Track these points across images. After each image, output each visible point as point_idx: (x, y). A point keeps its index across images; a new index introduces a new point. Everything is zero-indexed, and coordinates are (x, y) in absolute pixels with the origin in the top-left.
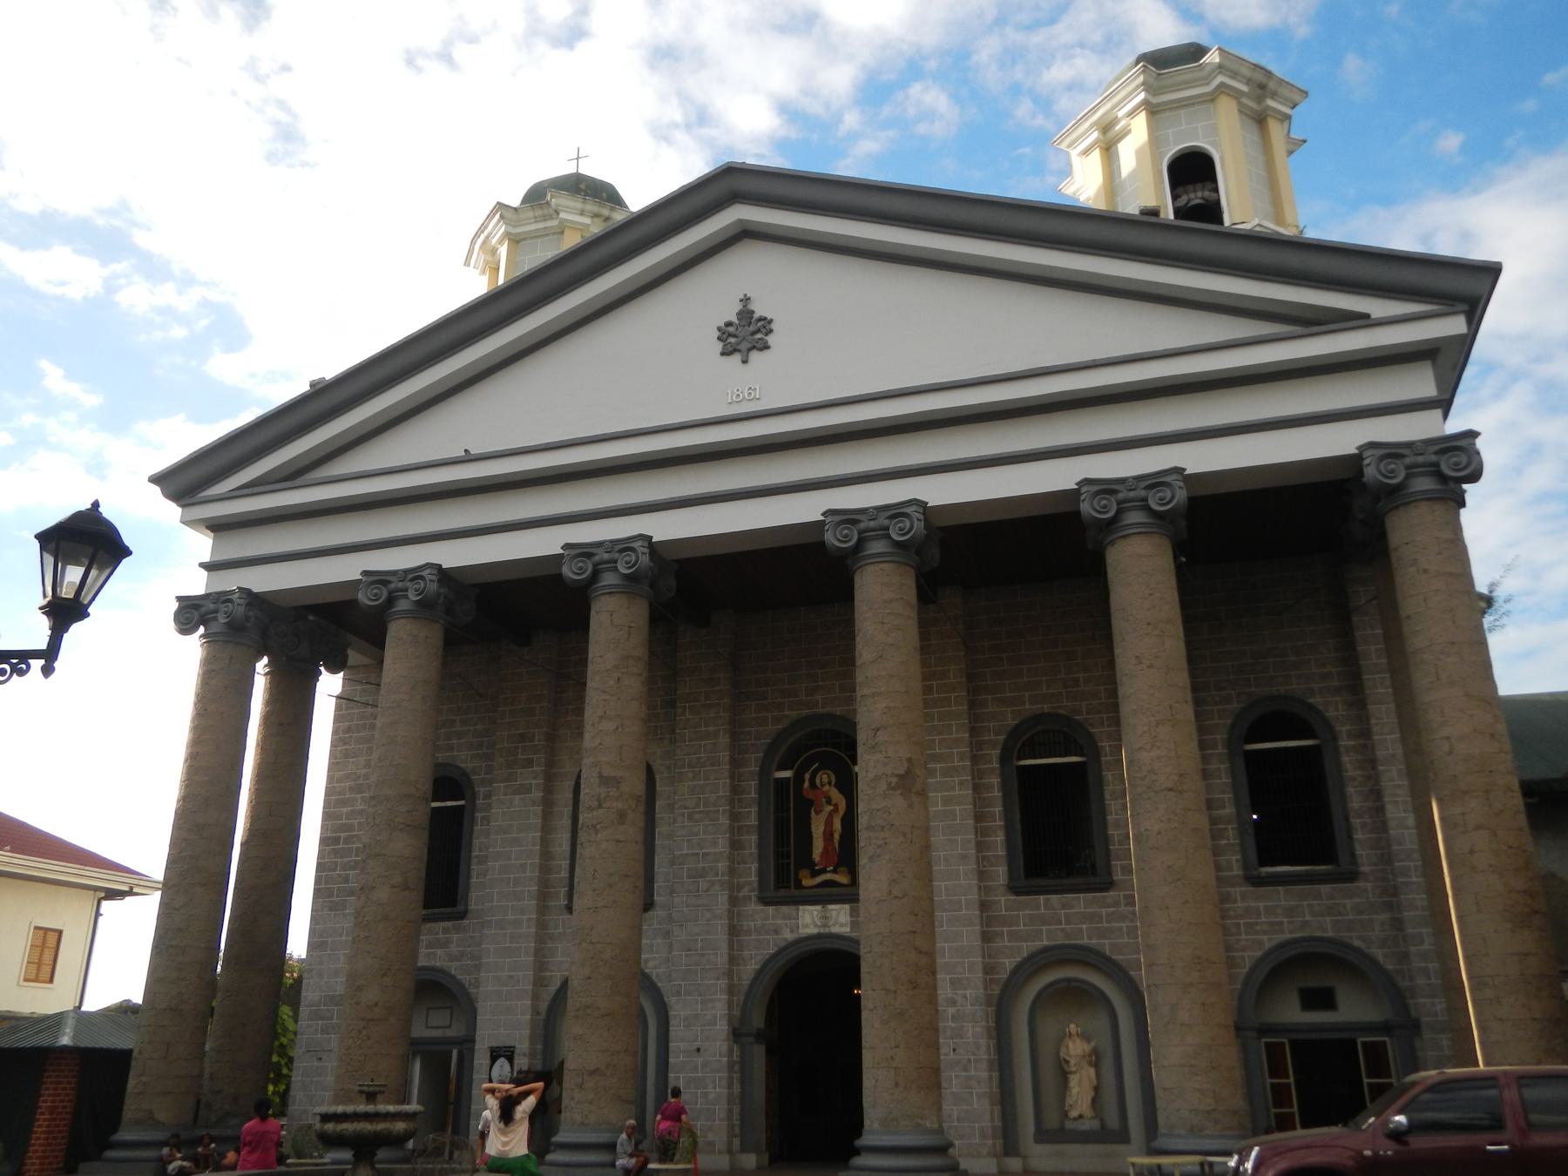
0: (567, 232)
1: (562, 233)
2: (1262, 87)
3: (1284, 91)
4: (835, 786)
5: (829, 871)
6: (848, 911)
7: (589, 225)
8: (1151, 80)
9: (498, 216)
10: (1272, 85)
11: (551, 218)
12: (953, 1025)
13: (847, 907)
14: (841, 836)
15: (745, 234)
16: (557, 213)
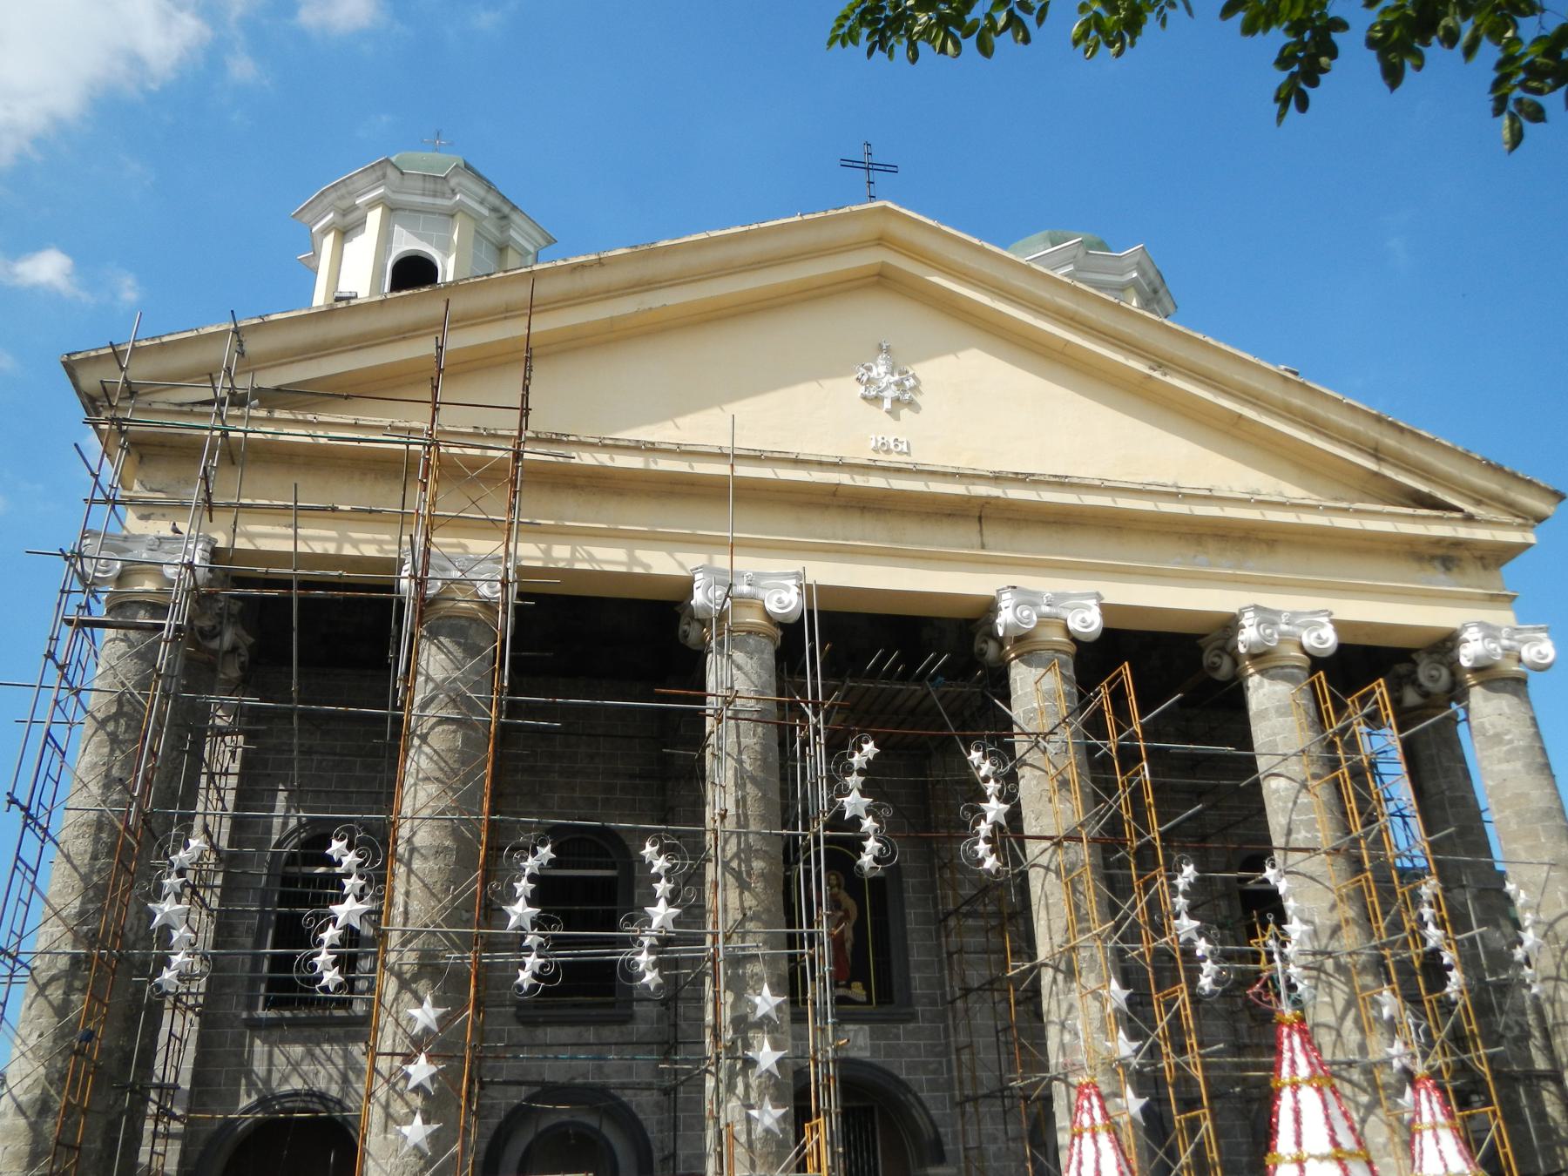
0: (459, 217)
1: (453, 216)
2: (1155, 291)
3: (1166, 300)
4: (846, 890)
5: (842, 986)
6: (868, 1033)
7: (486, 217)
8: (1081, 253)
9: (379, 173)
10: (1161, 292)
11: (443, 195)
12: (995, 1165)
13: (866, 1027)
14: (854, 946)
15: (882, 280)
16: (454, 193)
